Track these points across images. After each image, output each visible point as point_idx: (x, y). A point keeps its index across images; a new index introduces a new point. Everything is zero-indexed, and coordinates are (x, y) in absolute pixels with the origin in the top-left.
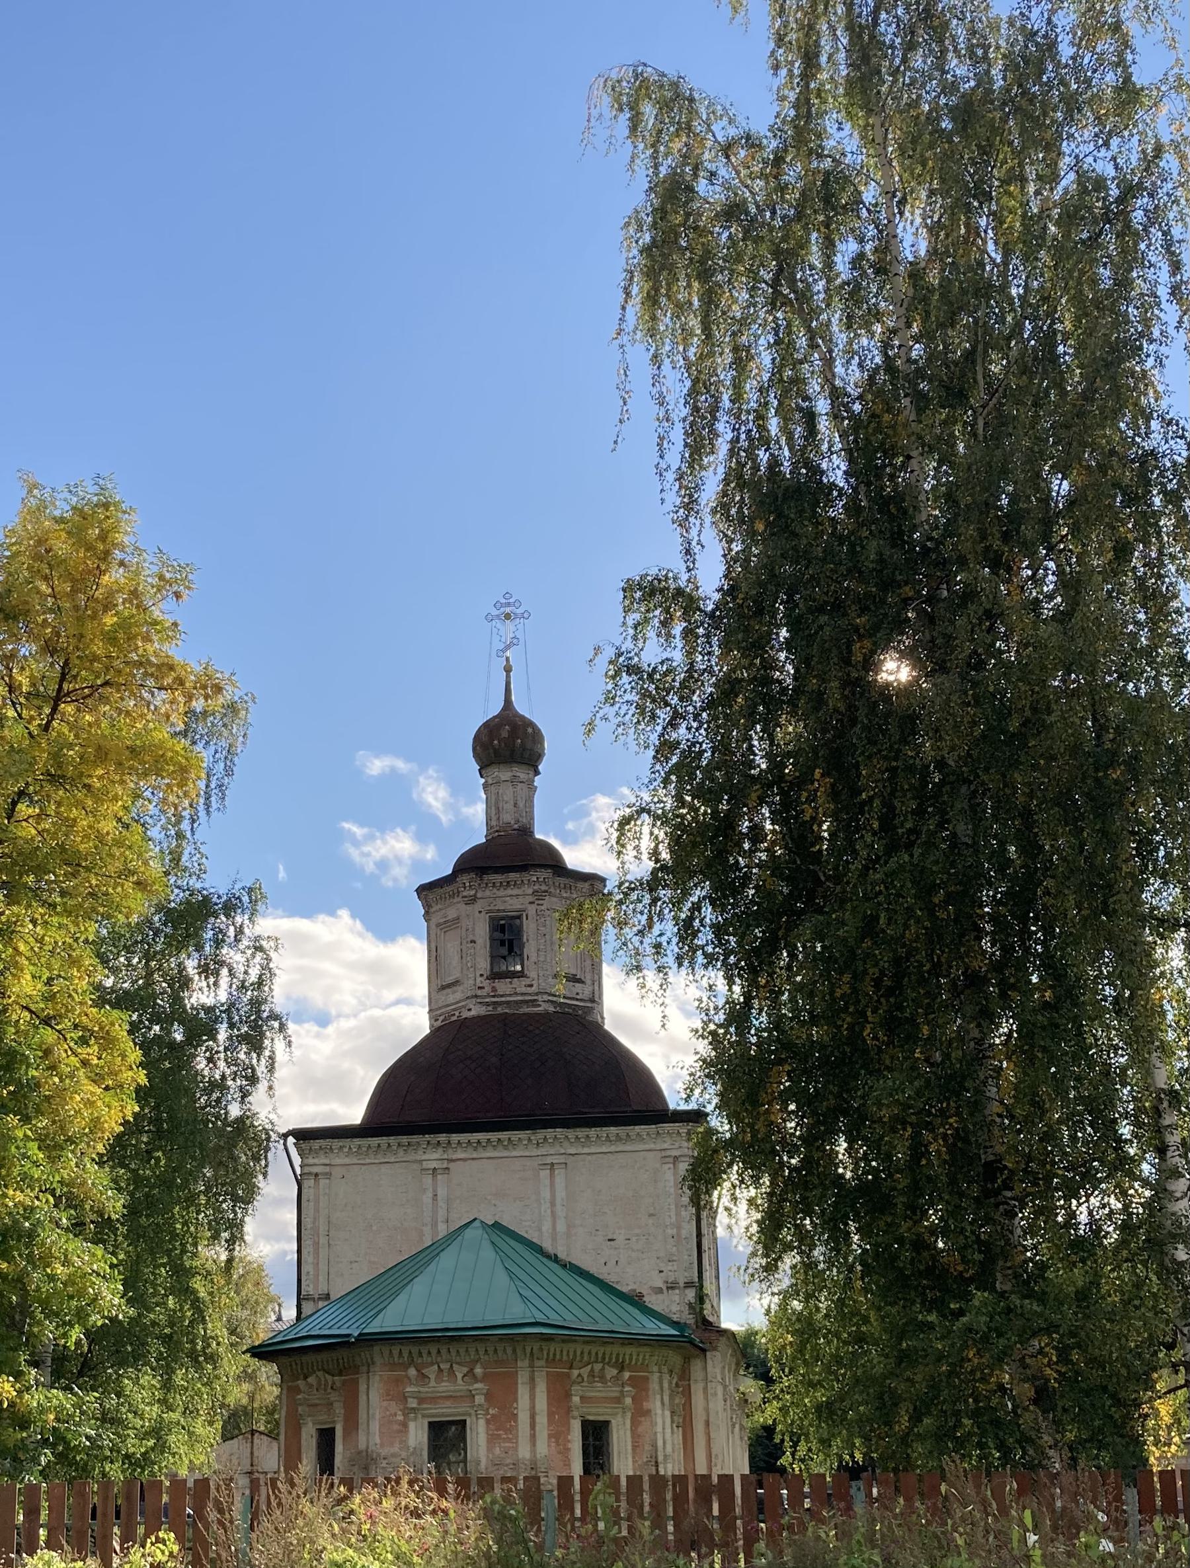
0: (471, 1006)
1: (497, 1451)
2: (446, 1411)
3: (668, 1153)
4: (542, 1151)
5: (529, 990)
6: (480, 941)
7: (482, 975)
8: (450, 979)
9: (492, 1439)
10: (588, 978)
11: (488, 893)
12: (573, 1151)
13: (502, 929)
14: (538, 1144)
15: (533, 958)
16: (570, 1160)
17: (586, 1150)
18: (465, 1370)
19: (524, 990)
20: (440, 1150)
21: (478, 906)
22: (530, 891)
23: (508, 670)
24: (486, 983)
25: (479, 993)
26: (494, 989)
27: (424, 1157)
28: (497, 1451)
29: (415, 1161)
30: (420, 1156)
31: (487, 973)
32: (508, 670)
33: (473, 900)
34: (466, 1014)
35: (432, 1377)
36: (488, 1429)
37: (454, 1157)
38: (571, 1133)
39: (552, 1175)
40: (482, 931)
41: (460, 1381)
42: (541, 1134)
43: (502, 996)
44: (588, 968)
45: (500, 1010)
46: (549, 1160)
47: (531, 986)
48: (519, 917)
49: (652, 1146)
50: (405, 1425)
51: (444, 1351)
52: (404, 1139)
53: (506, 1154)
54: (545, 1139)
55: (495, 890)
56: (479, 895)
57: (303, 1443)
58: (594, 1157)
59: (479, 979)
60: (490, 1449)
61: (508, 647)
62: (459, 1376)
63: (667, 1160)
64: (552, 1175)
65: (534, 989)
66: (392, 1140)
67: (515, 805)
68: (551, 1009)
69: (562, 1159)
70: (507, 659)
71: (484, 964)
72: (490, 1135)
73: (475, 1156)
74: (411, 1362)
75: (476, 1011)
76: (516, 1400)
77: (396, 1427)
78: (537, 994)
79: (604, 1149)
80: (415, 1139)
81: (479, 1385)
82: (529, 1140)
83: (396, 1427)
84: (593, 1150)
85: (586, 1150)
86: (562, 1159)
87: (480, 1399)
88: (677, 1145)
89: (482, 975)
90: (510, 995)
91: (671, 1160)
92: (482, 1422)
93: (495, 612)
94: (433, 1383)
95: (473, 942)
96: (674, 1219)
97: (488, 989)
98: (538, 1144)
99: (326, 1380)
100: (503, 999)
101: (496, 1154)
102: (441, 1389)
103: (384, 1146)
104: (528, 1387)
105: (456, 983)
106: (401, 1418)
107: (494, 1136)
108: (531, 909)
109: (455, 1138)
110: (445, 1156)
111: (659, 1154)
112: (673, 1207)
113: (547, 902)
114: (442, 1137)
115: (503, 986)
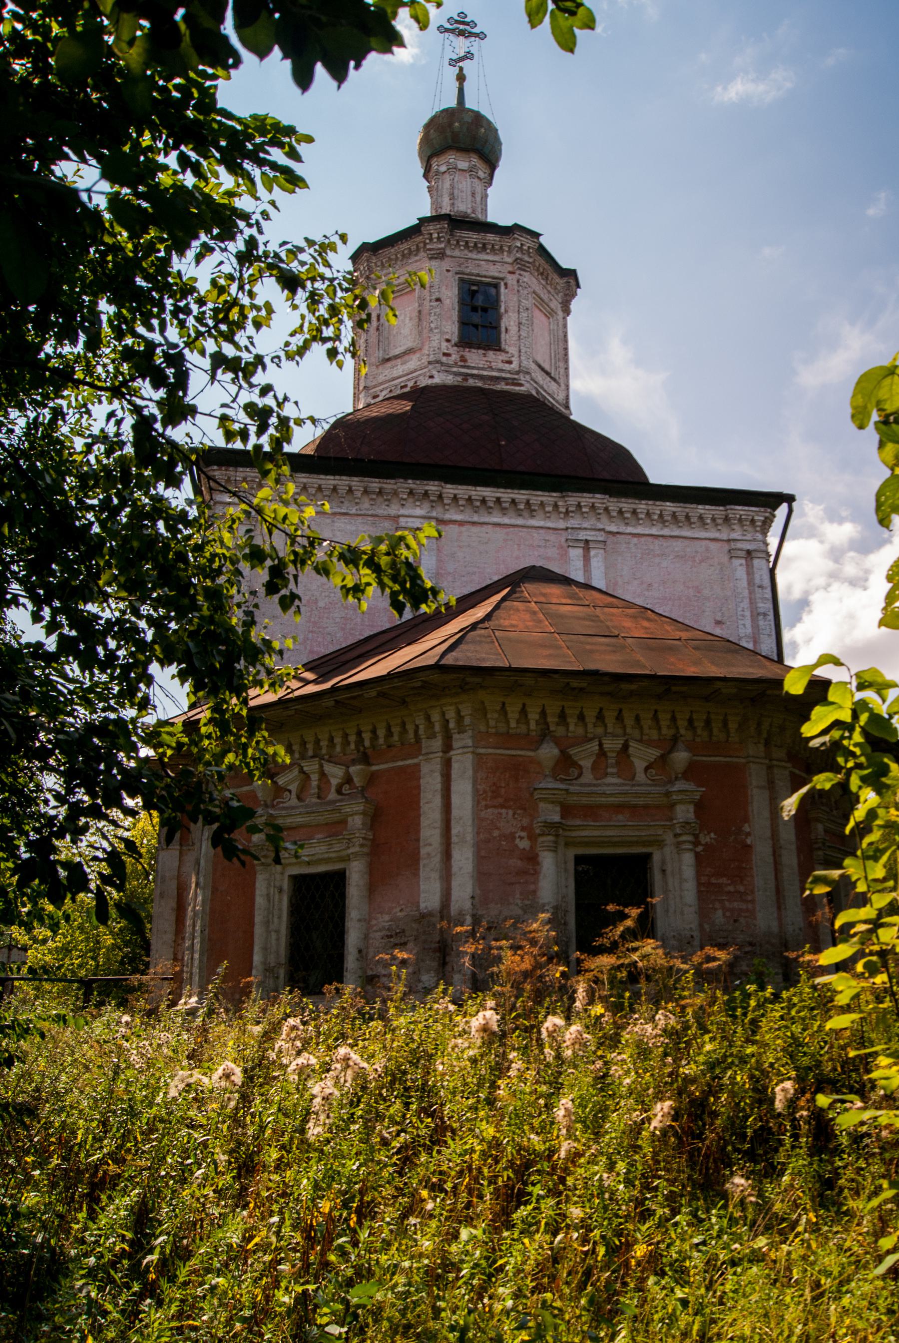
0: (435, 373)
1: (719, 917)
2: (610, 835)
3: (739, 545)
4: (573, 522)
5: (507, 367)
6: (447, 302)
7: (448, 341)
8: (397, 351)
9: (707, 892)
10: (562, 381)
11: (457, 253)
12: (613, 528)
13: (473, 294)
14: (567, 513)
15: (513, 329)
16: (611, 539)
17: (630, 530)
18: (654, 753)
19: (501, 366)
20: (426, 505)
21: (446, 264)
22: (510, 260)
23: (461, 78)
24: (453, 350)
25: (444, 359)
26: (463, 359)
27: (402, 512)
28: (719, 917)
29: (388, 517)
30: (394, 510)
31: (455, 339)
32: (461, 78)
33: (440, 255)
34: (424, 382)
35: (586, 764)
36: (698, 874)
37: (447, 516)
38: (614, 504)
39: (587, 559)
40: (450, 295)
41: (641, 777)
42: (573, 499)
43: (473, 368)
44: (562, 371)
45: (471, 382)
46: (582, 535)
47: (510, 362)
48: (496, 286)
49: (716, 535)
50: (532, 859)
51: (610, 716)
52: (375, 484)
53: (520, 521)
54: (579, 506)
55: (466, 252)
56: (448, 252)
57: (260, 901)
58: (643, 539)
59: (444, 344)
60: (703, 913)
61: (461, 59)
62: (639, 765)
63: (740, 553)
64: (587, 559)
65: (515, 366)
66: (356, 482)
67: (473, 194)
68: (534, 393)
69: (601, 537)
70: (461, 69)
71: (452, 328)
72: (500, 493)
73: (476, 518)
74: (545, 734)
75: (440, 379)
76: (746, 819)
77: (516, 863)
78: (518, 373)
79: (654, 531)
80: (389, 485)
81: (680, 785)
82: (556, 506)
83: (516, 863)
84: (639, 530)
85: (630, 530)
86: (601, 537)
87: (684, 812)
88: (749, 537)
89: (448, 341)
90: (483, 369)
91: (743, 554)
92: (688, 859)
93: (448, 26)
94: (588, 777)
95: (438, 300)
96: (749, 630)
97: (455, 357)
98: (567, 513)
99: (323, 775)
100: (475, 372)
101: (506, 520)
102: (608, 790)
103: (342, 491)
104: (766, 794)
105: (410, 351)
106: (524, 844)
107: (506, 495)
108: (511, 280)
109: (450, 490)
110: (434, 514)
111: (726, 547)
112: (748, 613)
113: (527, 277)
114: (433, 487)
115: (475, 358)
